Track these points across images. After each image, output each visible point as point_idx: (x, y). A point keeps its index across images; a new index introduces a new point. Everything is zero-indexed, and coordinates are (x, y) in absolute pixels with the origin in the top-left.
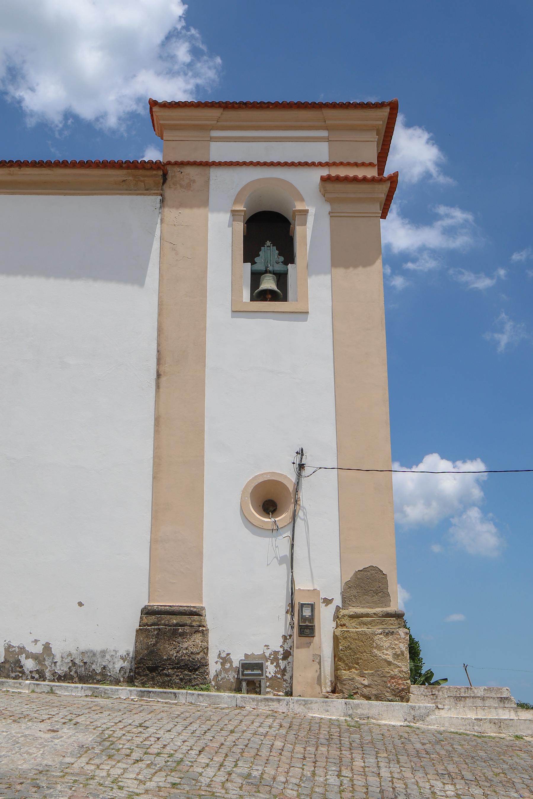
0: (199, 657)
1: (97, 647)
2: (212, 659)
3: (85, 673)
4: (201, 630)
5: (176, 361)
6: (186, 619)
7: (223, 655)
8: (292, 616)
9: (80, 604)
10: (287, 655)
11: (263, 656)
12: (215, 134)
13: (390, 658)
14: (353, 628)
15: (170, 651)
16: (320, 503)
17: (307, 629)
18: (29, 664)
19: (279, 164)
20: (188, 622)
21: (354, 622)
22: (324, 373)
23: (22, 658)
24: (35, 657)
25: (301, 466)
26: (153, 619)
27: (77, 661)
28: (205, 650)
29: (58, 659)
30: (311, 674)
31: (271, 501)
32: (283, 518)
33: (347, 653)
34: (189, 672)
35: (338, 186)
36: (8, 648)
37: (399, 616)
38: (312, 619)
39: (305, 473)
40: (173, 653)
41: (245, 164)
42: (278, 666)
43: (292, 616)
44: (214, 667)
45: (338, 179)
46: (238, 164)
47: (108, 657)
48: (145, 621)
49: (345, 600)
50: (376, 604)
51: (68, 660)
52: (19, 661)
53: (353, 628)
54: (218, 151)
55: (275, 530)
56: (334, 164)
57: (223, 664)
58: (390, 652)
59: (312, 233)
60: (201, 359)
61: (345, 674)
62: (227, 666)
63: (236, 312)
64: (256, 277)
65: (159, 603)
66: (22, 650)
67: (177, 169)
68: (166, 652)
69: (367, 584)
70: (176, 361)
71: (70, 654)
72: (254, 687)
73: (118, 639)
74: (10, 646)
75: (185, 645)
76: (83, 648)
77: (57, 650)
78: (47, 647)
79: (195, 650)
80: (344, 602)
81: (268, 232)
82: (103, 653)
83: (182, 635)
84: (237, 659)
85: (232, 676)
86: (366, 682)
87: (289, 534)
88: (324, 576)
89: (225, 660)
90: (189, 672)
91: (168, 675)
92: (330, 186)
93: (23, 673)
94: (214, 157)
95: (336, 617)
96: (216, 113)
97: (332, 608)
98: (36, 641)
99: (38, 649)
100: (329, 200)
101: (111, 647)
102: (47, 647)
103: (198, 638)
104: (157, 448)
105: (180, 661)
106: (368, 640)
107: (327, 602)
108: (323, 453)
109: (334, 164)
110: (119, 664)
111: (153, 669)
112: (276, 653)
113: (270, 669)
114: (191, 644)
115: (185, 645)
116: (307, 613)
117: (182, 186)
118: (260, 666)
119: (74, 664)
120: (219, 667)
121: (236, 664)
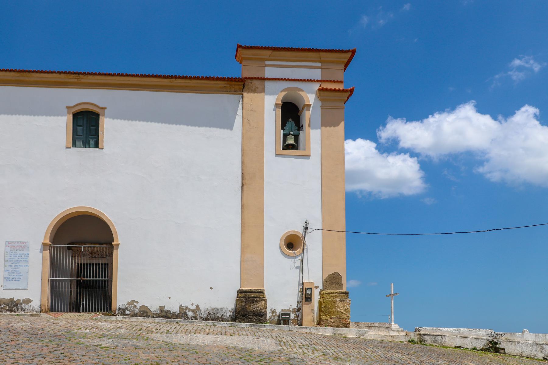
0: (263, 310)
1: (219, 307)
2: (268, 310)
3: (214, 317)
4: (264, 299)
6: (257, 295)
7: (273, 310)
8: (302, 294)
9: (211, 288)
10: (299, 310)
11: (289, 310)
12: (267, 63)
13: (343, 311)
14: (328, 298)
15: (251, 308)
16: (314, 245)
17: (308, 299)
18: (190, 314)
19: (298, 80)
20: (258, 296)
21: (328, 296)
22: (317, 185)
23: (187, 311)
24: (193, 311)
25: (307, 228)
26: (243, 295)
27: (211, 312)
28: (266, 308)
29: (202, 312)
30: (310, 318)
31: (292, 243)
32: (298, 251)
33: (324, 309)
35: (326, 93)
36: (181, 307)
37: (346, 293)
38: (311, 295)
39: (308, 231)
40: (252, 309)
41: (282, 79)
42: (296, 314)
43: (302, 294)
44: (269, 315)
45: (327, 90)
46: (279, 79)
47: (224, 311)
48: (240, 295)
49: (324, 287)
50: (337, 289)
51: (207, 312)
52: (186, 313)
53: (328, 298)
54: (269, 72)
55: (295, 257)
56: (324, 81)
57: (272, 314)
58: (343, 308)
60: (262, 178)
61: (323, 317)
62: (274, 314)
63: (277, 155)
64: (285, 137)
65: (245, 288)
66: (187, 308)
67: (249, 81)
68: (249, 308)
69: (333, 280)
71: (207, 310)
72: (286, 323)
73: (227, 303)
74: (181, 306)
75: (258, 306)
76: (213, 307)
77: (202, 308)
78: (197, 307)
79: (262, 308)
80: (323, 287)
81: (291, 113)
82: (222, 309)
83: (256, 301)
84: (278, 311)
85: (276, 319)
86: (332, 321)
88: (315, 277)
89: (273, 312)
91: (250, 318)
92: (322, 93)
93: (188, 317)
94: (267, 75)
95: (320, 294)
96: (269, 52)
97: (318, 290)
98: (193, 304)
99: (194, 307)
101: (225, 306)
102: (197, 307)
103: (263, 302)
104: (242, 219)
105: (255, 312)
106: (334, 303)
107: (317, 287)
108: (316, 223)
109: (324, 81)
110: (229, 314)
111: (243, 316)
112: (295, 309)
113: (293, 316)
114: (259, 305)
115: (258, 306)
116: (309, 292)
117: (252, 90)
118: (289, 314)
119: (209, 314)
120: (271, 315)
121: (278, 313)
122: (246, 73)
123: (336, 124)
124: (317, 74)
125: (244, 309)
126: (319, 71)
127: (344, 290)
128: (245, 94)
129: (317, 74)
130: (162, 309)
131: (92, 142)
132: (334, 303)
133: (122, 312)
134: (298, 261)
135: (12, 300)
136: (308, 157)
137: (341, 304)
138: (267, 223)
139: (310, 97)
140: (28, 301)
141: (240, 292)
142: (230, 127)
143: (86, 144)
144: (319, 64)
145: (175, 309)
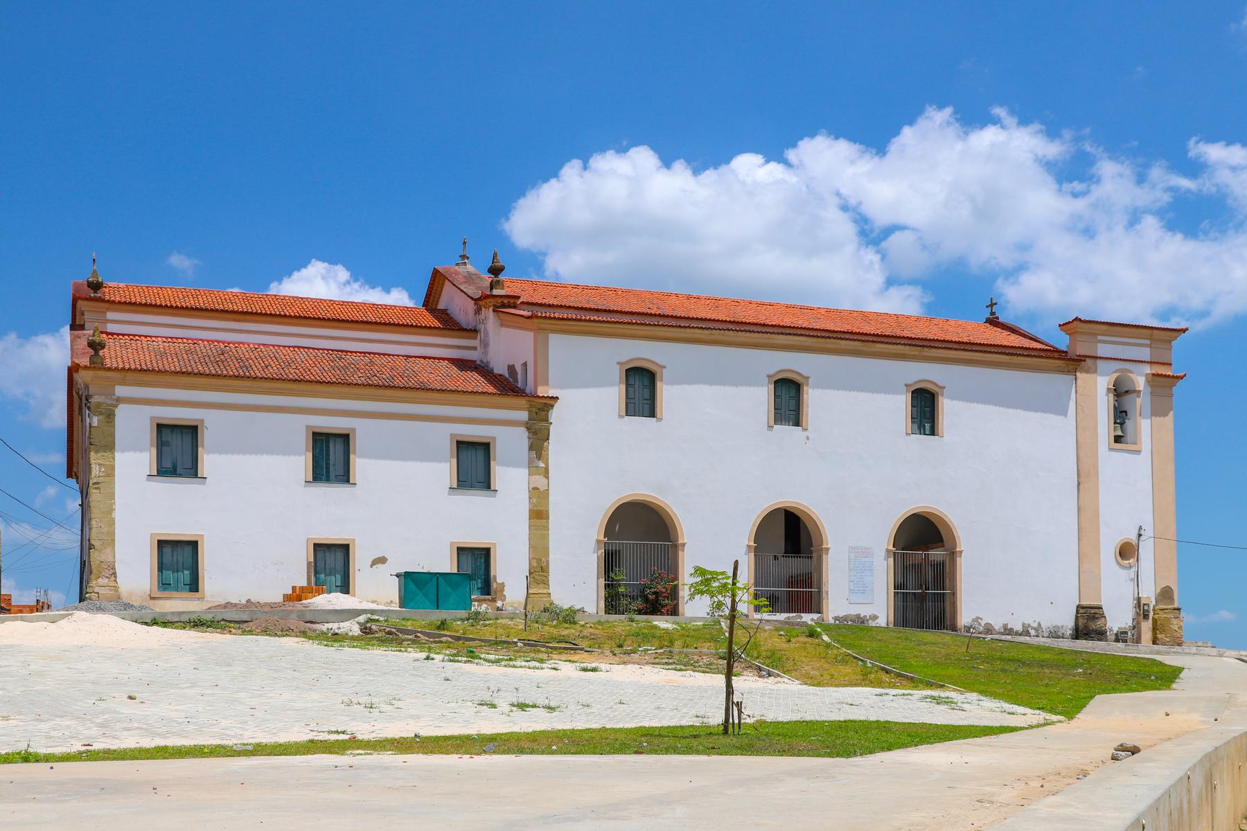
3: (1054, 634)
5: (1085, 477)
12: (1100, 338)
14: (1162, 615)
15: (1093, 626)
17: (1146, 617)
18: (1033, 632)
25: (1140, 535)
34: (1101, 635)
37: (1179, 609)
53: (1162, 615)
54: (1103, 350)
59: (1141, 403)
61: (1159, 636)
63: (1110, 449)
65: (1084, 603)
70: (1085, 477)
73: (1067, 621)
78: (1039, 624)
85: (1113, 637)
87: (1134, 569)
88: (1149, 593)
90: (1101, 635)
99: (1035, 625)
100: (1152, 386)
102: (1039, 624)
106: (1168, 620)
122: (1081, 350)
123: (1165, 414)
124: (1145, 354)
125: (1086, 627)
126: (1147, 350)
127: (1176, 606)
128: (1078, 374)
129: (1145, 354)
130: (1005, 626)
131: (927, 426)
132: (1168, 620)
133: (968, 629)
134: (1132, 572)
135: (858, 616)
136: (1138, 452)
137: (1175, 621)
138: (1103, 529)
139: (1140, 382)
140: (875, 617)
141: (1079, 607)
142: (1064, 413)
143: (921, 430)
144: (1148, 342)
145: (1019, 628)
